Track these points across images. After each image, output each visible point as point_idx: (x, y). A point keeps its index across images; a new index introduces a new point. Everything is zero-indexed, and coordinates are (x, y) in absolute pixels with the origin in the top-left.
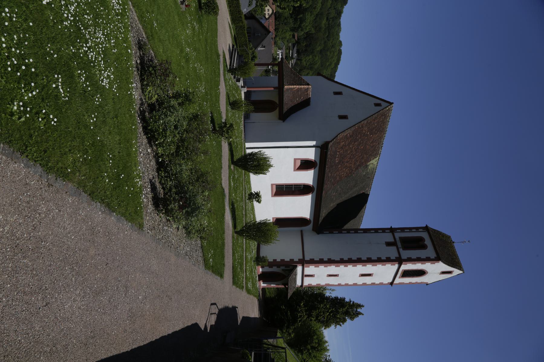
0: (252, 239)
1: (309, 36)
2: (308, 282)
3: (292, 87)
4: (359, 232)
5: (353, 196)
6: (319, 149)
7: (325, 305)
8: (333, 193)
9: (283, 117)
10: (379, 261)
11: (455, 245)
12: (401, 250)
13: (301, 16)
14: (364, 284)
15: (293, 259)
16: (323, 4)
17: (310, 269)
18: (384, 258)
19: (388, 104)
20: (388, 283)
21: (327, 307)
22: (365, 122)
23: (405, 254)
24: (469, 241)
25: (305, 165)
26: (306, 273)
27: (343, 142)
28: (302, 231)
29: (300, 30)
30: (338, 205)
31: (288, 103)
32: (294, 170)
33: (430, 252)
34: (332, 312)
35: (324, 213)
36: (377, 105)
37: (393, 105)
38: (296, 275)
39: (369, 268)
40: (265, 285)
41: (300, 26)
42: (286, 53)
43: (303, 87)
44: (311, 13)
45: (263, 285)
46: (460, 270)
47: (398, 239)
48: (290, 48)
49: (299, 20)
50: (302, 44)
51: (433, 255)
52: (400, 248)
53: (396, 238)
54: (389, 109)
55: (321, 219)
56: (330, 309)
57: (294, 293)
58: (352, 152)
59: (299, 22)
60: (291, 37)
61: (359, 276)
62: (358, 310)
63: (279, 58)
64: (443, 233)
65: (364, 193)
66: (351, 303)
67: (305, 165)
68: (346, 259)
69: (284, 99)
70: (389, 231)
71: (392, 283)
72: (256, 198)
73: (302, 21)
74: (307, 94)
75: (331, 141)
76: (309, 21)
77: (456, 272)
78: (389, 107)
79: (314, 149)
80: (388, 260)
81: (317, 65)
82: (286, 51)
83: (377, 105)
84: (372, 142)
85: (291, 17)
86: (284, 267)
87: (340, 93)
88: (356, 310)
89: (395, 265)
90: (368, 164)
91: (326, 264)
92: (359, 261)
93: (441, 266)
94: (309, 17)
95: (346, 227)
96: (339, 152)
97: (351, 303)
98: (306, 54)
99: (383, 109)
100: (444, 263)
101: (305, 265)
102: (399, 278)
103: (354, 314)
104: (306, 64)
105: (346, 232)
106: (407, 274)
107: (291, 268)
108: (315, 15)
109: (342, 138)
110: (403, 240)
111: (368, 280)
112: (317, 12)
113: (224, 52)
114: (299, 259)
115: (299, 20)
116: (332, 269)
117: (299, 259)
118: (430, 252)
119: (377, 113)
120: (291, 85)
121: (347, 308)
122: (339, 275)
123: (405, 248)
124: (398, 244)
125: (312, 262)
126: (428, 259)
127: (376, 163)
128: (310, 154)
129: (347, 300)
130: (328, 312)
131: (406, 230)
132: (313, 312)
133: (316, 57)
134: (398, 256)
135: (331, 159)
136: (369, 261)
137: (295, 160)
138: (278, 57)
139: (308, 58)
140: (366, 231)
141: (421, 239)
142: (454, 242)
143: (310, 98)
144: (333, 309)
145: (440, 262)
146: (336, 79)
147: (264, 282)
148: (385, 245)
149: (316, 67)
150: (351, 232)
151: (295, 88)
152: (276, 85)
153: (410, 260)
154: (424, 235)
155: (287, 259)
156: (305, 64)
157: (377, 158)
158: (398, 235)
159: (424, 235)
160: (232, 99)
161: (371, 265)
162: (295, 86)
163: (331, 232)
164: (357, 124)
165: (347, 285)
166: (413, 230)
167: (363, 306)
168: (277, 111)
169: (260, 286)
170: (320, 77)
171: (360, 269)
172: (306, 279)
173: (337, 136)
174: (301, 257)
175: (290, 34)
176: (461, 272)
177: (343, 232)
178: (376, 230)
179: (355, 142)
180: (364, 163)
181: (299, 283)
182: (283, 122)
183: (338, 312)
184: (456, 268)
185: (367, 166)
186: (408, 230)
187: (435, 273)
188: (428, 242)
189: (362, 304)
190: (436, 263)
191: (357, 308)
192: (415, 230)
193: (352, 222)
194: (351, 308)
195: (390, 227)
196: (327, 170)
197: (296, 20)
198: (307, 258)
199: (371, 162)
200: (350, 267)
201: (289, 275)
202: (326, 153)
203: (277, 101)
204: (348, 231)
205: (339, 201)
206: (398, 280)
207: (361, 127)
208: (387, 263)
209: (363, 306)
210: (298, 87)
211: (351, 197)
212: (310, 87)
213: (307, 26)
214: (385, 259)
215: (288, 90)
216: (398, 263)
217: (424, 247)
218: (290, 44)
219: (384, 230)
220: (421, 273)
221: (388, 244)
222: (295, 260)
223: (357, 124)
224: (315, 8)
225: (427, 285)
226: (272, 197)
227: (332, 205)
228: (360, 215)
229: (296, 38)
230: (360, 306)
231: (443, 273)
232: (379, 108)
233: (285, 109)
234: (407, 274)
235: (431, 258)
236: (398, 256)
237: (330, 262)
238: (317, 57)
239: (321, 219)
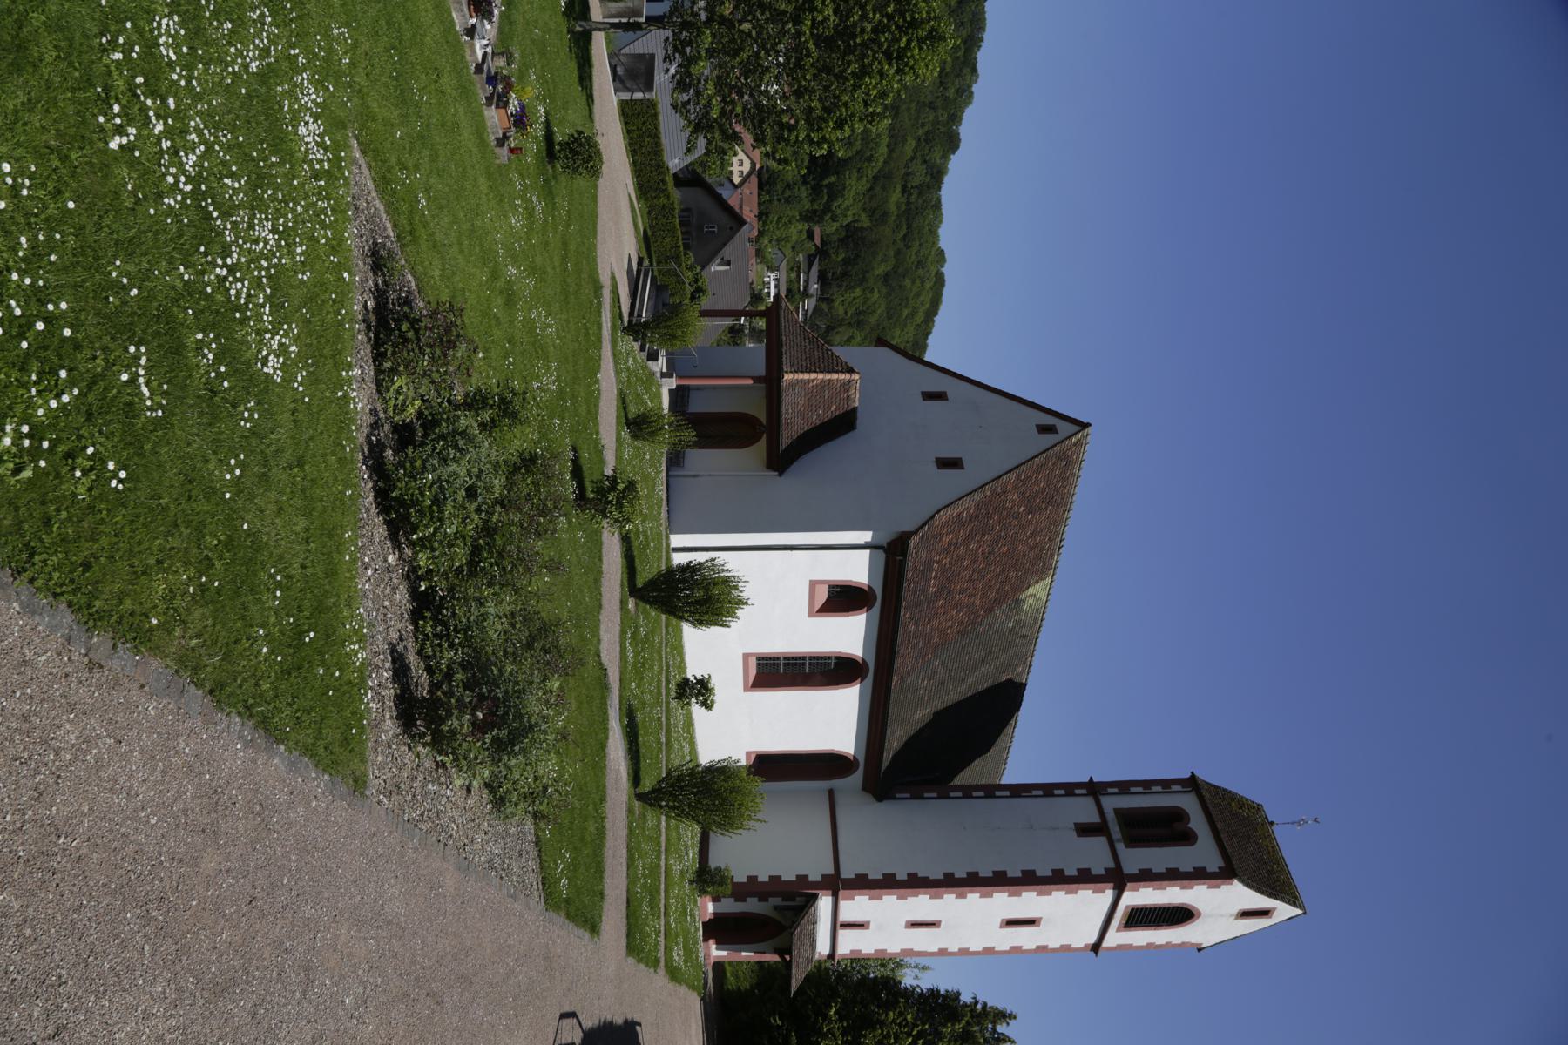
0: (687, 816)
1: (852, 236)
2: (849, 943)
3: (806, 376)
4: (998, 793)
5: (980, 688)
6: (881, 555)
7: (901, 1014)
8: (923, 680)
9: (780, 461)
10: (1059, 879)
12: (1120, 847)
13: (833, 179)
14: (1016, 950)
15: (806, 877)
16: (891, 150)
17: (856, 906)
18: (1071, 871)
19: (1074, 428)
20: (1086, 945)
21: (905, 1019)
22: (1013, 476)
23: (1134, 859)
24: (1315, 820)
25: (842, 599)
26: (844, 916)
27: (948, 534)
28: (831, 793)
29: (828, 217)
30: (938, 715)
31: (795, 418)
32: (811, 615)
33: (1205, 852)
34: (920, 1035)
35: (896, 738)
36: (1045, 429)
37: (1089, 430)
38: (814, 923)
39: (1028, 902)
40: (724, 953)
41: (827, 209)
42: (789, 282)
43: (835, 376)
44: (858, 172)
45: (716, 953)
46: (1294, 904)
47: (1110, 816)
48: (799, 267)
49: (825, 191)
51: (1214, 862)
52: (1118, 841)
53: (1105, 811)
54: (1079, 440)
55: (888, 756)
56: (915, 1025)
57: (808, 979)
58: (974, 561)
59: (826, 198)
60: (804, 236)
61: (1001, 927)
62: (1001, 1028)
63: (769, 294)
64: (1242, 797)
65: (1010, 681)
66: (979, 1007)
67: (842, 599)
68: (960, 874)
69: (783, 410)
70: (1084, 791)
71: (1096, 947)
72: (700, 693)
73: (835, 192)
74: (848, 397)
75: (916, 532)
76: (852, 193)
77: (1284, 911)
78: (1079, 435)
79: (867, 553)
80: (1085, 878)
81: (876, 316)
82: (788, 276)
83: (1045, 429)
84: (1033, 535)
85: (805, 183)
86: (780, 899)
87: (939, 396)
88: (994, 1030)
89: (1104, 892)
90: (1023, 596)
91: (902, 891)
93: (1238, 895)
94: (853, 183)
95: (959, 780)
96: (937, 562)
97: (979, 1007)
98: (845, 284)
99: (1062, 441)
100: (1247, 885)
101: (841, 892)
102: (1118, 930)
104: (846, 313)
105: (960, 794)
106: (1141, 918)
107: (799, 901)
108: (870, 176)
109: (947, 522)
110: (1126, 817)
111: (1026, 938)
112: (875, 171)
113: (613, 278)
114: (823, 876)
115: (825, 191)
116: (922, 905)
117: (823, 876)
118: (1205, 852)
119: (1044, 452)
120: (802, 372)
121: (968, 1023)
122: (943, 924)
123: (1133, 841)
124: (1112, 832)
125: (862, 883)
126: (1199, 875)
127: (1045, 593)
128: (857, 569)
129: (966, 998)
130: (909, 1034)
131: (1133, 790)
132: (865, 1036)
133: (872, 291)
134: (1112, 865)
135: (916, 583)
136: (1029, 879)
137: (813, 584)
138: (766, 290)
139: (849, 296)
140: (1019, 791)
141: (1179, 815)
142: (1272, 823)
143: (855, 409)
144: (924, 1024)
145: (1236, 881)
146: (928, 357)
147: (721, 944)
148: (1075, 833)
149: (873, 319)
150: (975, 794)
151: (813, 380)
152: (762, 371)
153: (1147, 877)
155: (788, 876)
156: (841, 311)
157: (1048, 580)
158: (1111, 803)
160: (633, 410)
161: (1035, 893)
162: (813, 376)
163: (917, 796)
164: (989, 483)
165: (964, 952)
166: (1155, 789)
167: (1012, 1016)
168: (763, 443)
169: (707, 955)
171: (1004, 903)
172: (843, 934)
173: (933, 516)
174: (830, 871)
175: (800, 227)
176: (1298, 911)
177: (952, 794)
178: (1048, 790)
179: (984, 535)
180: (1010, 594)
181: (823, 948)
182: (780, 475)
184: (1282, 900)
185: (1018, 603)
186: (1140, 789)
187: (1222, 916)
188: (1198, 823)
189: (1009, 1012)
190: (1223, 887)
191: (994, 1023)
192: (1159, 789)
193: (977, 764)
194: (979, 1024)
195: (1087, 780)
196: (904, 614)
197: (816, 190)
198: (847, 873)
199: (1031, 591)
200: (974, 898)
201: (794, 924)
202: (902, 565)
203: (763, 417)
204: (967, 792)
205: (938, 705)
206: (1114, 938)
207: (999, 491)
208: (1081, 885)
209: (1012, 1016)
210: (821, 376)
211: (973, 692)
212: (857, 377)
213: (848, 209)
214: (1075, 873)
215: (792, 384)
216: (1112, 885)
217: (1188, 838)
218: (801, 257)
219: (1069, 789)
220: (1180, 915)
221: (1084, 830)
222: (811, 879)
223: (989, 483)
224: (869, 159)
225: (1199, 950)
226: (746, 690)
227: (919, 715)
228: (999, 743)
229: (818, 241)
230: (1003, 1016)
231: (1246, 914)
232: (1049, 439)
233: (786, 439)
234: (1141, 918)
235: (1210, 869)
236: (1112, 865)
237: (915, 883)
238: (876, 294)
239: (888, 756)
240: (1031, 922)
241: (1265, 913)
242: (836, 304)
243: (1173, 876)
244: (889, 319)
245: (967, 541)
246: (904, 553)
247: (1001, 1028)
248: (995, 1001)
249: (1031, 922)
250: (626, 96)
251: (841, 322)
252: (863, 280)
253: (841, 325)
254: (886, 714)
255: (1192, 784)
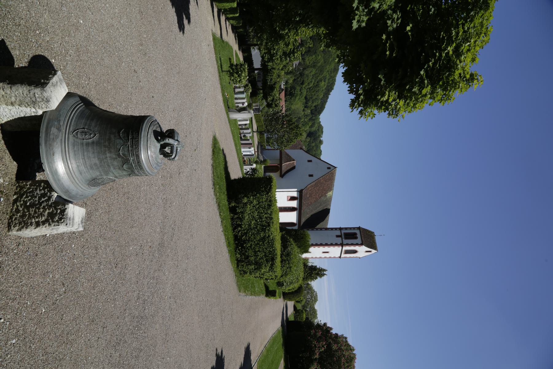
6: (299, 193)
9: (282, 176)
10: (332, 245)
11: (376, 237)
12: (343, 239)
14: (325, 257)
18: (334, 243)
19: (334, 168)
22: (322, 178)
23: (345, 241)
25: (292, 199)
30: (312, 215)
32: (287, 201)
34: (308, 273)
35: (303, 220)
36: (329, 168)
39: (326, 249)
50: (305, 45)
51: (360, 242)
55: (302, 223)
62: (325, 273)
67: (292, 199)
71: (340, 257)
77: (374, 251)
79: (296, 192)
80: (336, 245)
81: (320, 64)
83: (329, 168)
92: (321, 245)
98: (309, 54)
103: (321, 274)
104: (310, 63)
106: (347, 252)
111: (327, 255)
118: (359, 241)
123: (346, 238)
126: (357, 244)
127: (331, 194)
128: (295, 194)
129: (318, 267)
133: (319, 56)
136: (326, 245)
137: (288, 196)
139: (311, 58)
141: (355, 234)
143: (295, 166)
149: (319, 64)
152: (279, 163)
153: (347, 245)
154: (358, 232)
156: (308, 63)
158: (343, 232)
159: (358, 232)
166: (356, 229)
167: (327, 270)
168: (279, 171)
170: (302, 150)
171: (322, 249)
176: (376, 251)
178: (332, 229)
183: (312, 274)
184: (373, 249)
185: (326, 196)
191: (323, 271)
193: (321, 223)
195: (339, 227)
196: (303, 201)
200: (317, 248)
206: (343, 255)
209: (327, 270)
211: (318, 211)
215: (284, 165)
217: (356, 238)
219: (336, 229)
220: (355, 252)
221: (337, 236)
227: (308, 216)
230: (325, 270)
232: (329, 170)
233: (283, 173)
234: (347, 252)
236: (341, 242)
238: (320, 56)
240: (327, 252)
241: (370, 251)
242: (306, 60)
243: (352, 244)
244: (325, 63)
245: (314, 188)
246: (302, 192)
247: (325, 273)
248: (323, 267)
249: (327, 252)
250: (255, 113)
251: (308, 67)
252: (315, 53)
253: (308, 68)
254: (301, 216)
255: (359, 228)
